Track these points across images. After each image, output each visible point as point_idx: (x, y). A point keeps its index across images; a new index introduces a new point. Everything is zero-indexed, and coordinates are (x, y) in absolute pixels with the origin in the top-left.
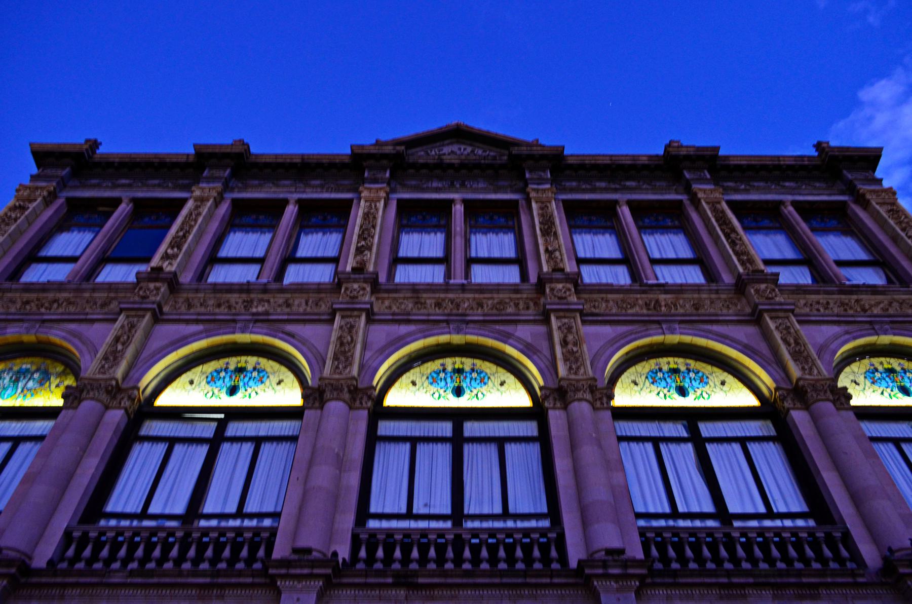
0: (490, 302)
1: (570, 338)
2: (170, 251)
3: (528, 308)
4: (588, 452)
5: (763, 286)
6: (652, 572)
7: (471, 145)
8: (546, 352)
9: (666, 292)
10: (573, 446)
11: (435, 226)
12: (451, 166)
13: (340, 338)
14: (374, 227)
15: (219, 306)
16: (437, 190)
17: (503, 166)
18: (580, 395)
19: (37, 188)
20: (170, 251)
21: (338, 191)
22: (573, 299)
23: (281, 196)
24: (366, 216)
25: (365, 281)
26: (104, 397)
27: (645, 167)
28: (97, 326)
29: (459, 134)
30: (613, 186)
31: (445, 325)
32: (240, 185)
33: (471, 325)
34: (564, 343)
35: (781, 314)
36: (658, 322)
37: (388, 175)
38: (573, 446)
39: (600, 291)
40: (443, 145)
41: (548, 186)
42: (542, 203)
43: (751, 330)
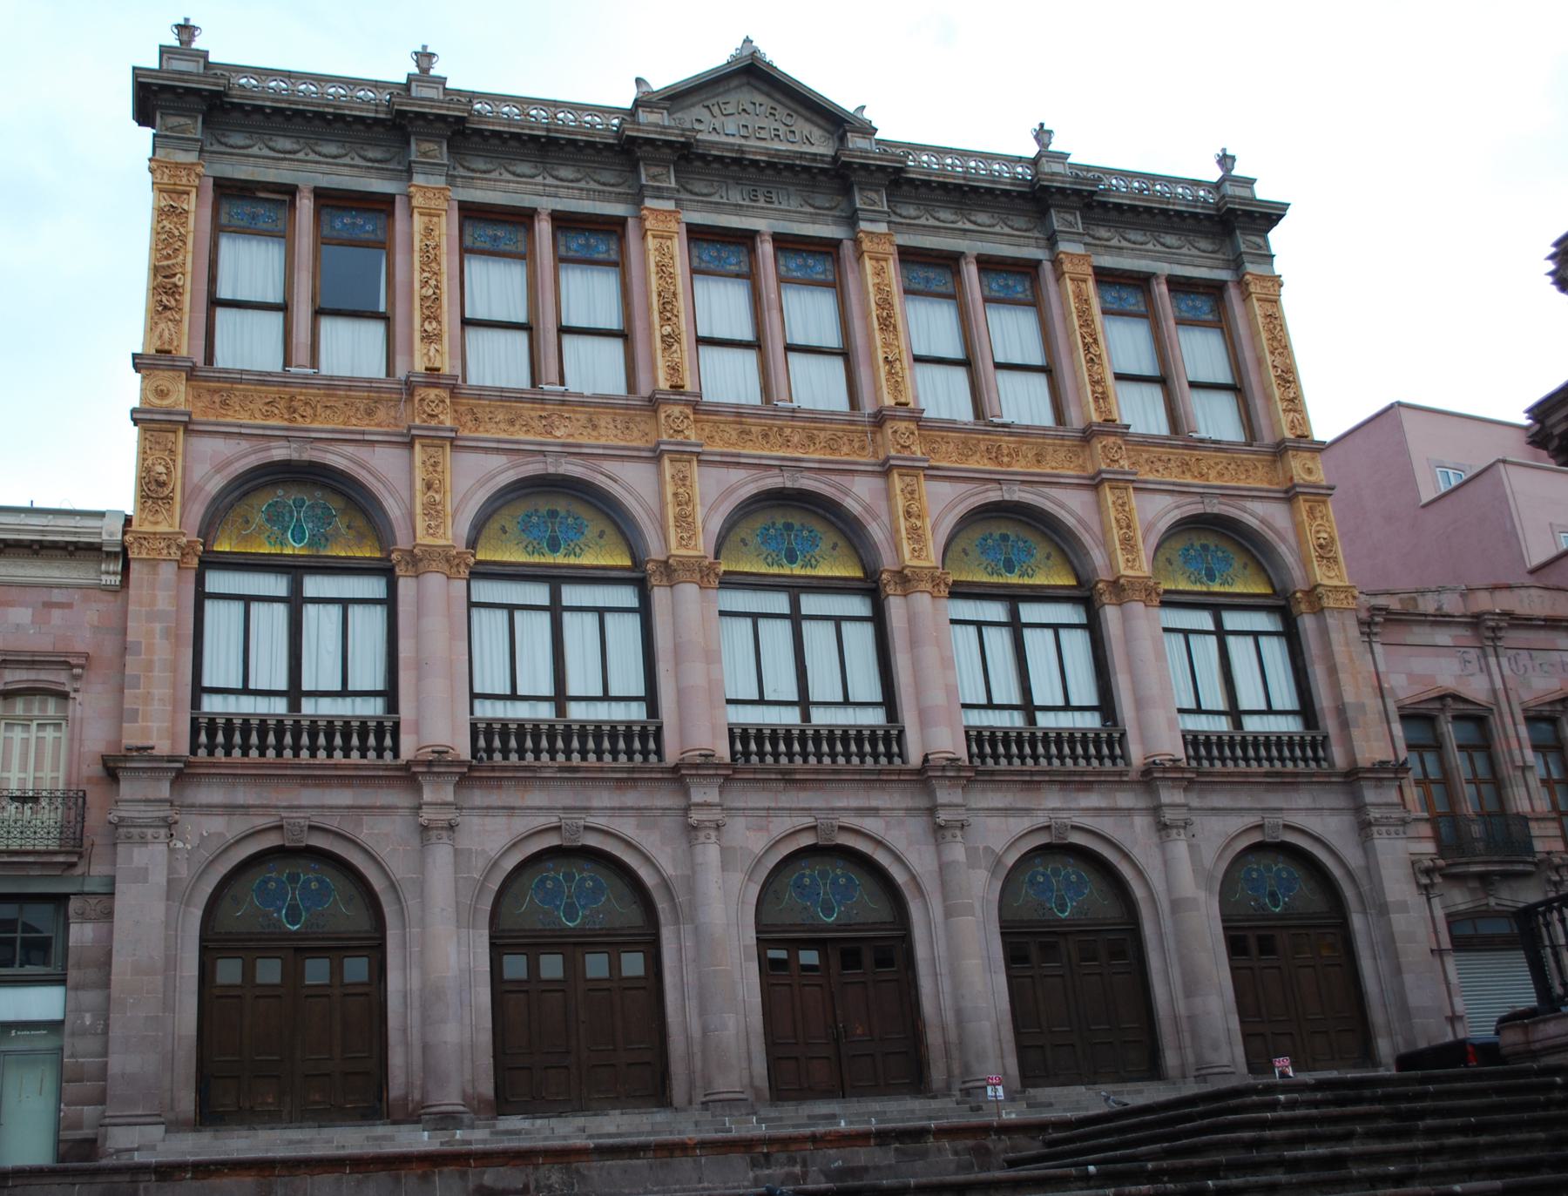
0: (822, 435)
1: (914, 509)
2: (427, 326)
3: (863, 448)
4: (930, 654)
5: (1112, 439)
6: (978, 773)
7: (768, 95)
8: (885, 518)
9: (1011, 434)
10: (914, 643)
11: (738, 276)
12: (755, 163)
13: (676, 495)
14: (674, 294)
15: (512, 423)
16: (737, 209)
17: (821, 170)
18: (922, 586)
19: (177, 165)
20: (427, 326)
21: (602, 196)
22: (918, 451)
23: (527, 201)
24: (661, 267)
25: (687, 403)
26: (446, 568)
27: (1006, 193)
28: (379, 449)
29: (751, 73)
30: (959, 225)
31: (777, 471)
32: (462, 172)
33: (806, 474)
34: (908, 514)
35: (1121, 484)
36: (998, 481)
37: (673, 184)
38: (914, 643)
39: (941, 429)
40: (727, 91)
41: (882, 228)
42: (878, 260)
43: (1087, 496)
